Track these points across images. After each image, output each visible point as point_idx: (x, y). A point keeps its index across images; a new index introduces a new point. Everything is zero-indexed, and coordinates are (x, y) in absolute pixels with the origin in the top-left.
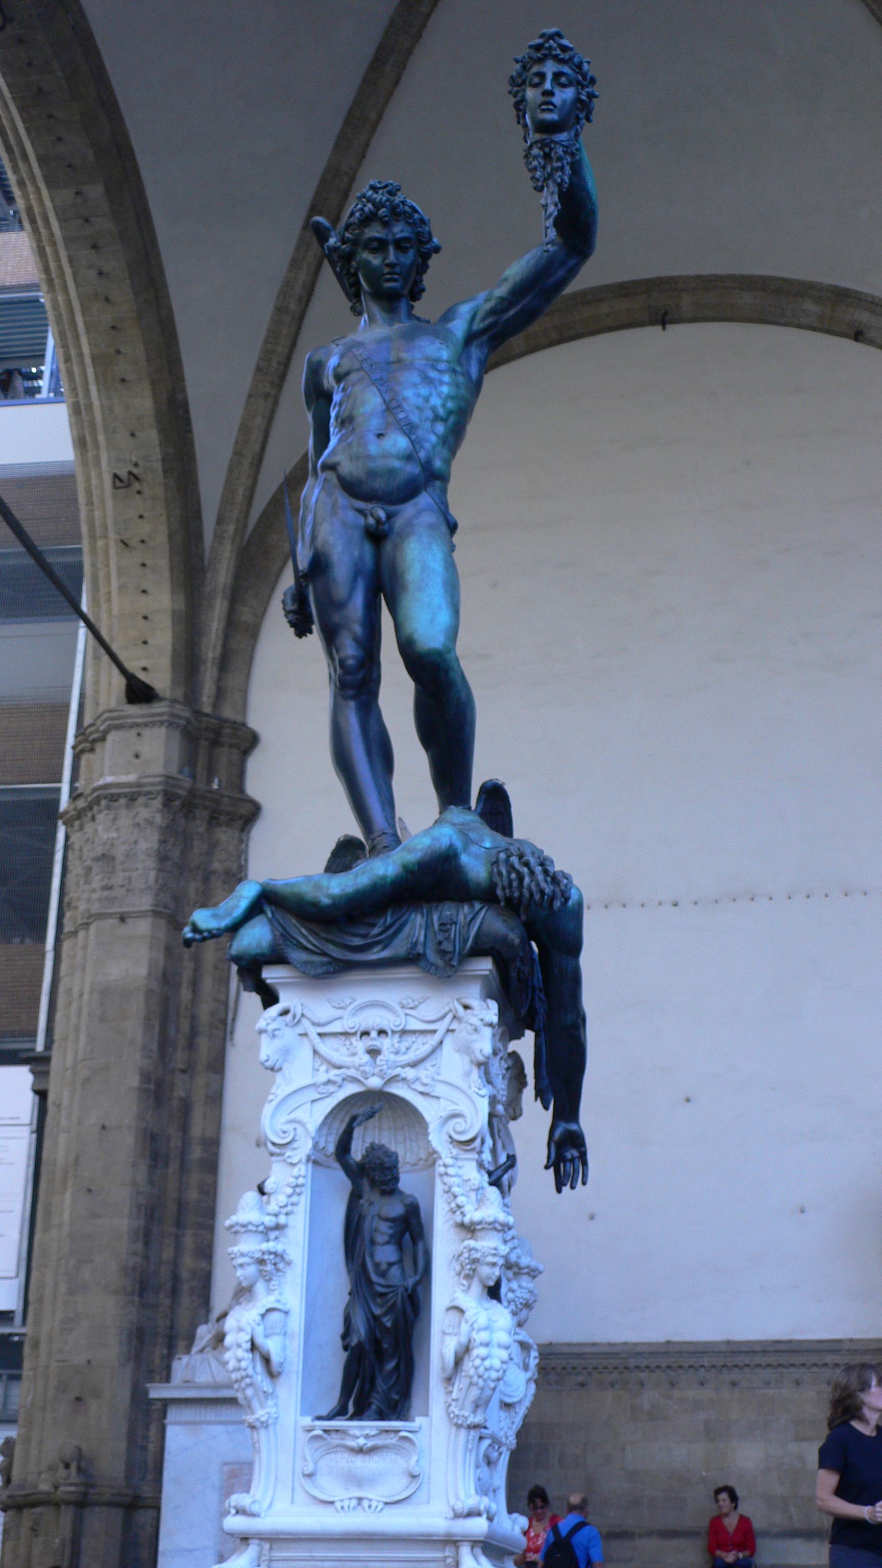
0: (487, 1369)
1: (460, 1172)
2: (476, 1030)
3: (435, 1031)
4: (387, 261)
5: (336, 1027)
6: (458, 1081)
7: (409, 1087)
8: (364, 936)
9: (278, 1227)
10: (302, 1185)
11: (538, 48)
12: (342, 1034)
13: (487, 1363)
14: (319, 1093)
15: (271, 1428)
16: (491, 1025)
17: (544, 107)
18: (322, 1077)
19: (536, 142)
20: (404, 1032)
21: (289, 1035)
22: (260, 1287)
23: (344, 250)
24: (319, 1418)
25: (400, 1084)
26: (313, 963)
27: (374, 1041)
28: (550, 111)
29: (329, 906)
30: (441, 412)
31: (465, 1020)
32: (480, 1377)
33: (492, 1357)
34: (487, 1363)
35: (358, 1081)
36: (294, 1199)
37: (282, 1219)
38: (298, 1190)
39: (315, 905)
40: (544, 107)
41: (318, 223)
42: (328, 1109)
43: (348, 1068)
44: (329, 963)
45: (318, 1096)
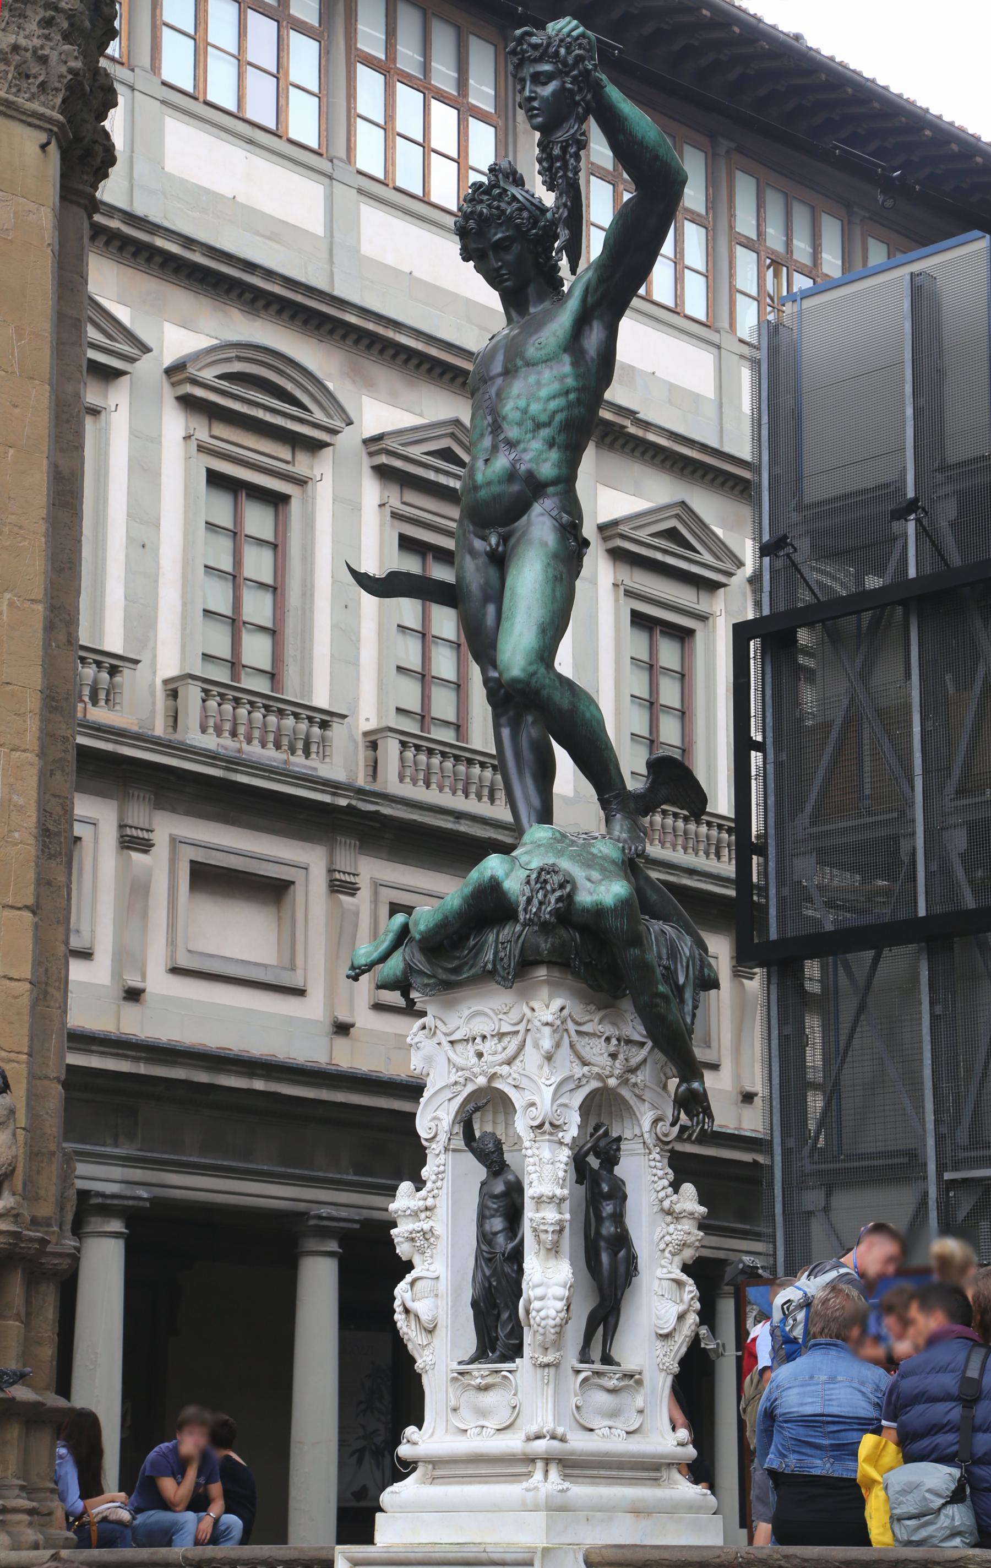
0: (543, 1319)
1: (537, 1152)
8: (458, 958)
9: (427, 1209)
10: (443, 1172)
13: (542, 1314)
15: (430, 1371)
16: (547, 1024)
18: (453, 1078)
21: (428, 1045)
22: (416, 1260)
24: (460, 1363)
27: (480, 1046)
30: (544, 418)
32: (539, 1325)
33: (548, 1308)
34: (542, 1314)
36: (439, 1184)
37: (430, 1202)
38: (440, 1176)
42: (458, 1106)
45: (451, 1096)
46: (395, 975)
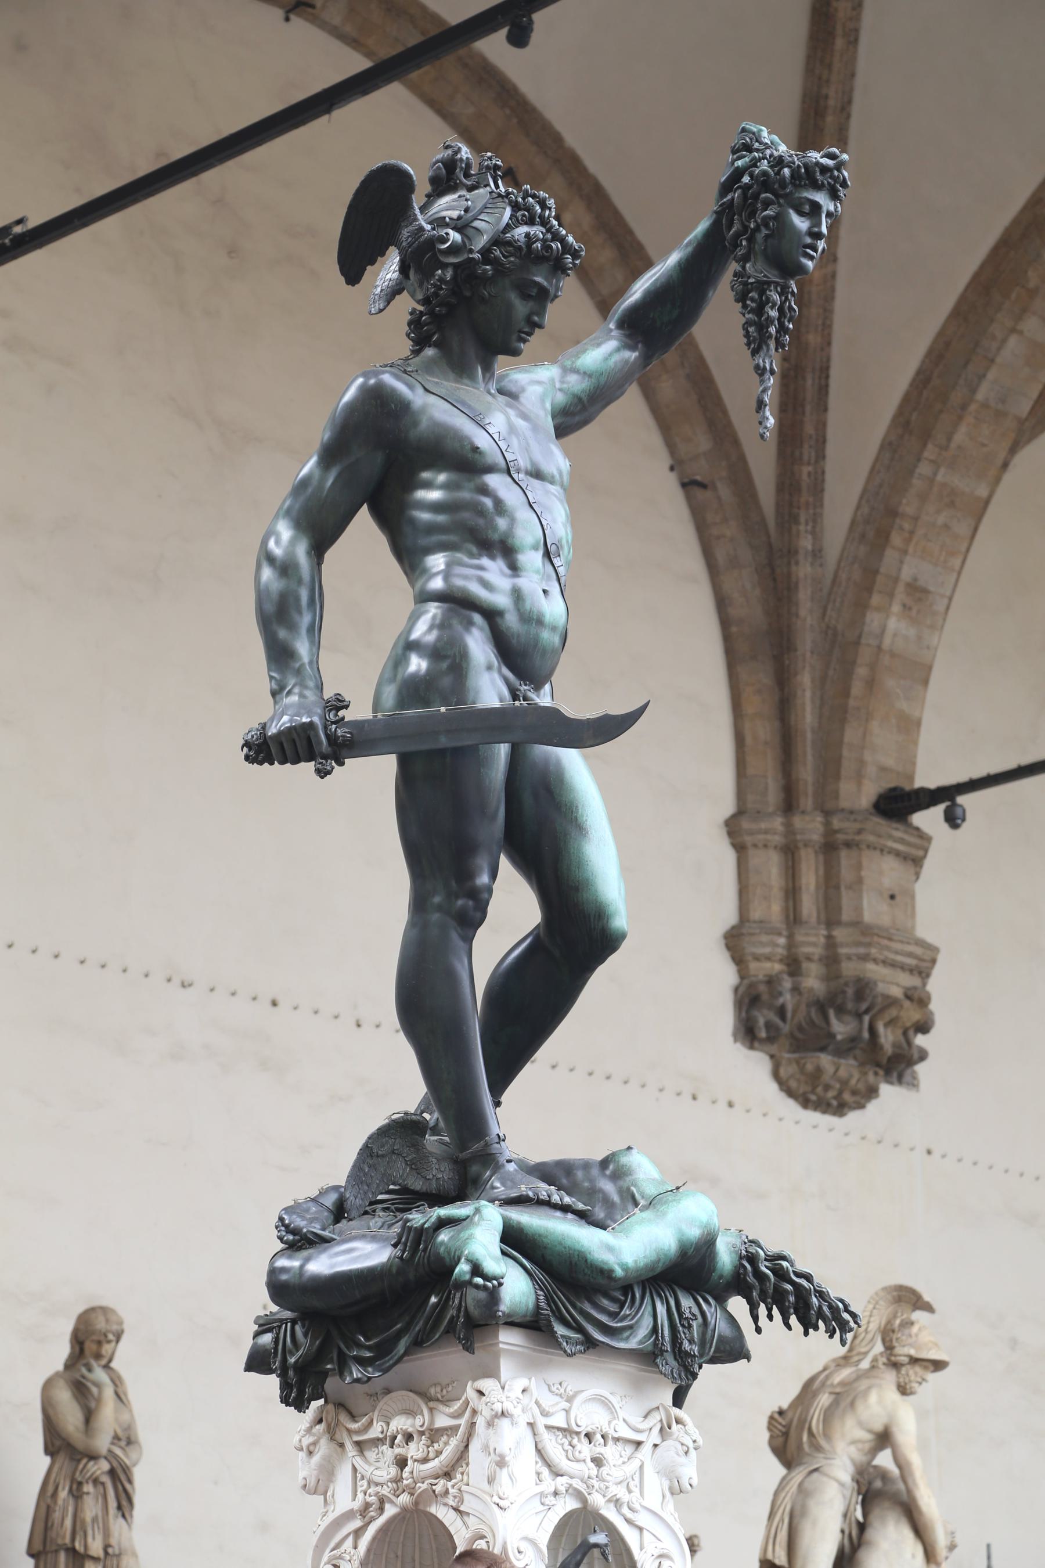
2: (686, 1453)
3: (639, 1444)
4: (536, 318)
5: (559, 1421)
6: (657, 1509)
7: (619, 1511)
8: (614, 1315)
11: (825, 170)
12: (559, 1429)
14: (542, 1504)
17: (808, 251)
19: (777, 284)
20: (617, 1440)
23: (485, 271)
25: (612, 1505)
26: (567, 1339)
27: (599, 1449)
28: (812, 258)
29: (620, 1279)
31: (675, 1436)
35: (579, 1495)
39: (606, 1273)
40: (808, 251)
41: (408, 176)
43: (572, 1478)
44: (582, 1344)
46: (527, 1306)
